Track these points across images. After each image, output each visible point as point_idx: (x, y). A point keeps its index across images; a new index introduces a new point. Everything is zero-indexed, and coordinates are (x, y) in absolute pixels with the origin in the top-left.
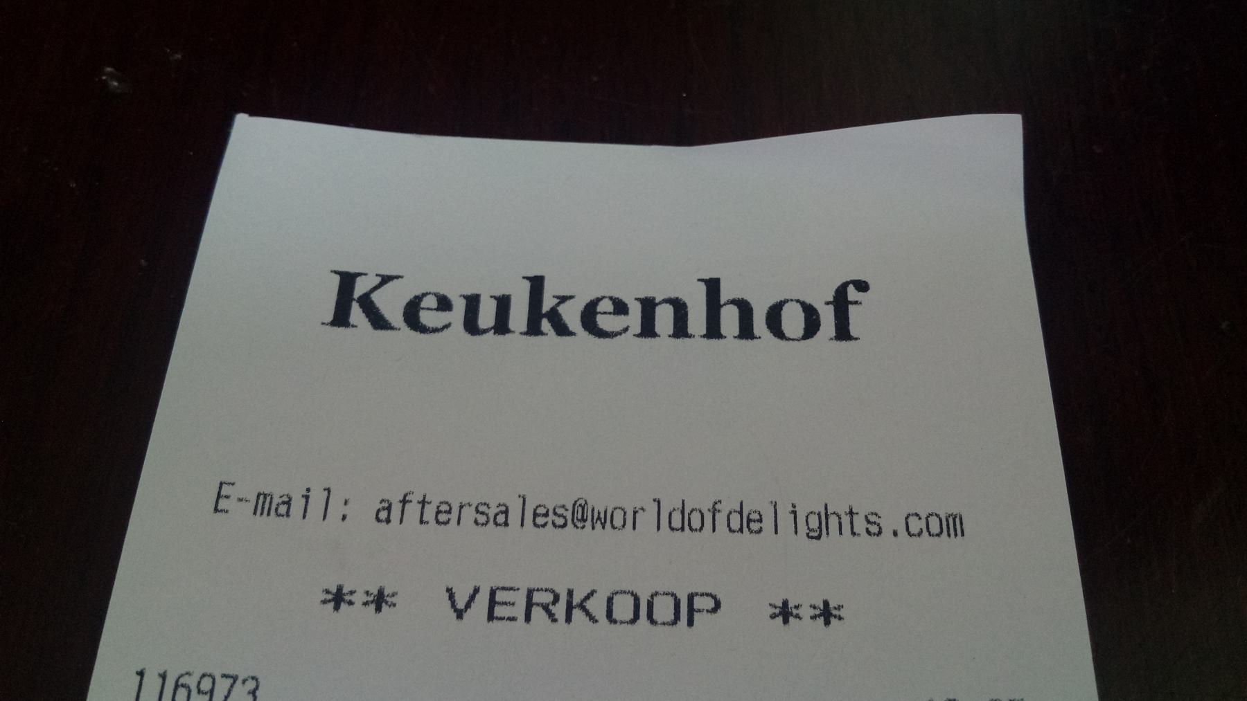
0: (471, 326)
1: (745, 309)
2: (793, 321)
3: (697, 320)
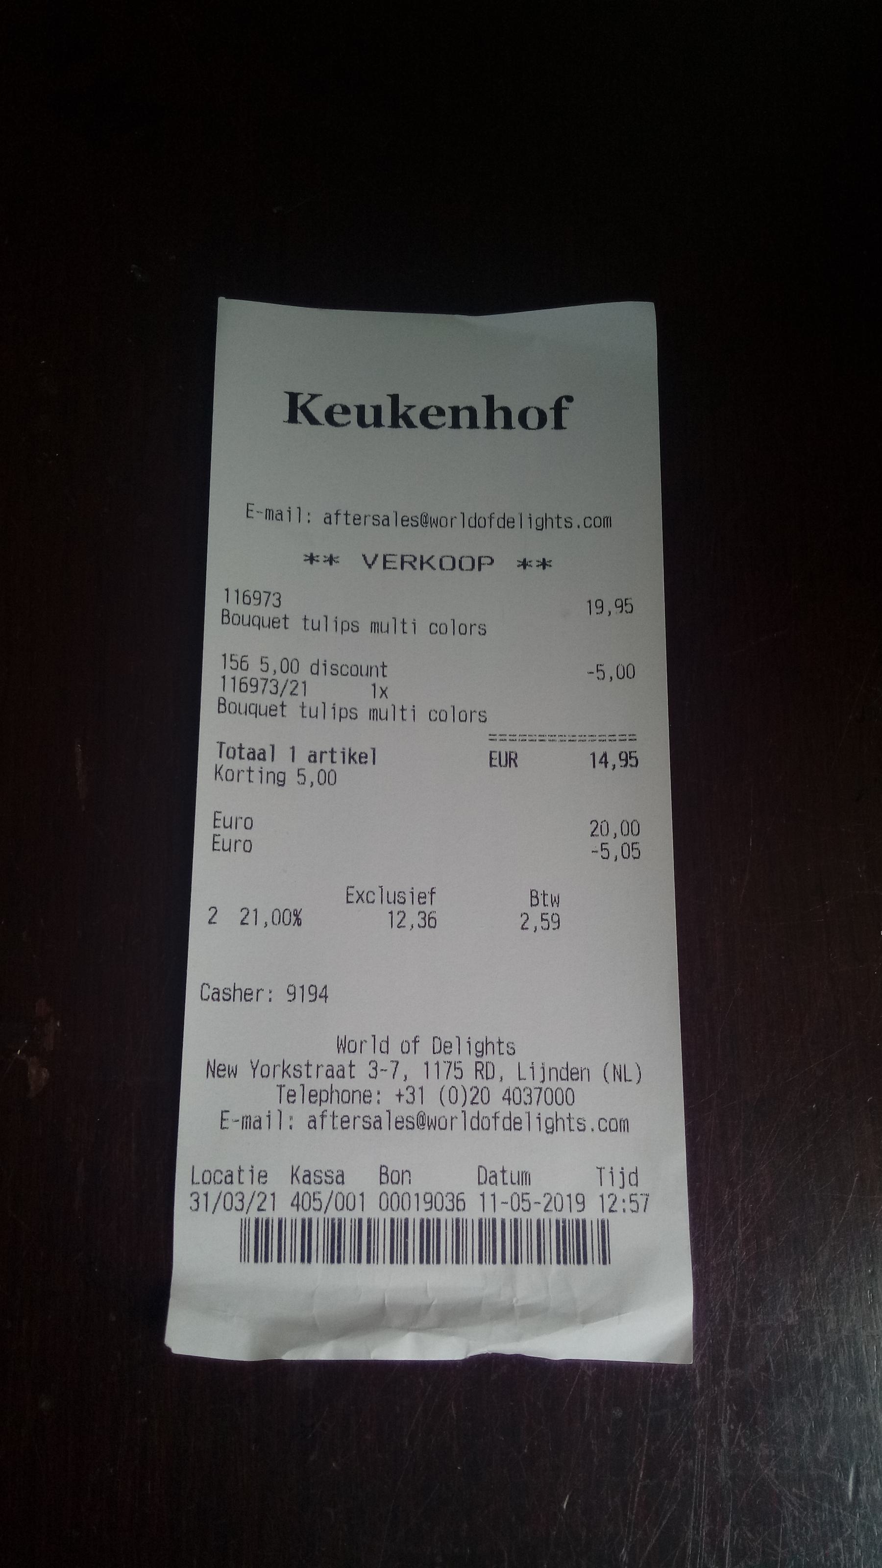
0: (361, 422)
1: (507, 412)
2: (533, 419)
3: (482, 420)
